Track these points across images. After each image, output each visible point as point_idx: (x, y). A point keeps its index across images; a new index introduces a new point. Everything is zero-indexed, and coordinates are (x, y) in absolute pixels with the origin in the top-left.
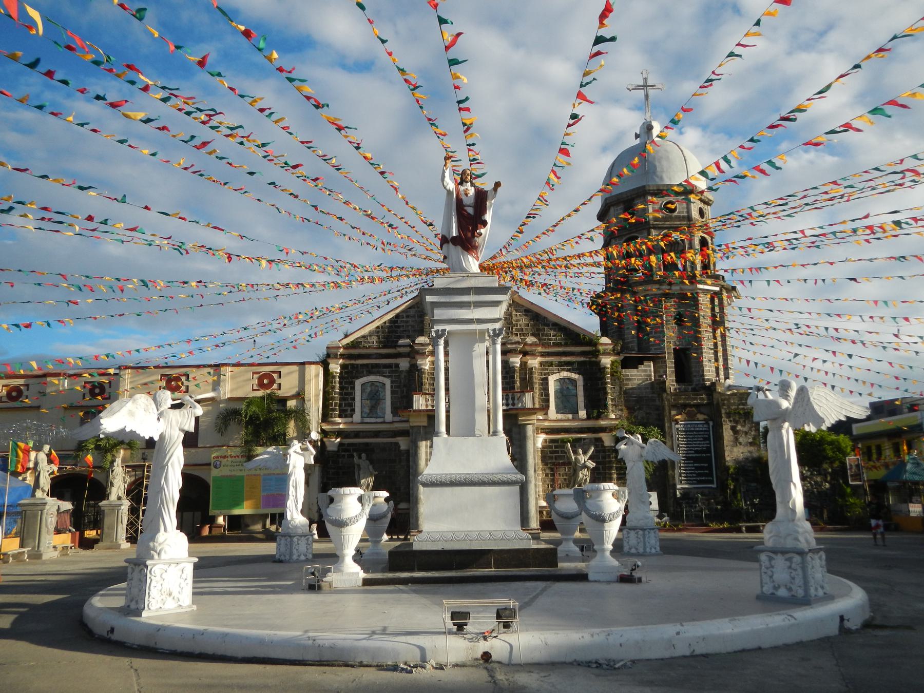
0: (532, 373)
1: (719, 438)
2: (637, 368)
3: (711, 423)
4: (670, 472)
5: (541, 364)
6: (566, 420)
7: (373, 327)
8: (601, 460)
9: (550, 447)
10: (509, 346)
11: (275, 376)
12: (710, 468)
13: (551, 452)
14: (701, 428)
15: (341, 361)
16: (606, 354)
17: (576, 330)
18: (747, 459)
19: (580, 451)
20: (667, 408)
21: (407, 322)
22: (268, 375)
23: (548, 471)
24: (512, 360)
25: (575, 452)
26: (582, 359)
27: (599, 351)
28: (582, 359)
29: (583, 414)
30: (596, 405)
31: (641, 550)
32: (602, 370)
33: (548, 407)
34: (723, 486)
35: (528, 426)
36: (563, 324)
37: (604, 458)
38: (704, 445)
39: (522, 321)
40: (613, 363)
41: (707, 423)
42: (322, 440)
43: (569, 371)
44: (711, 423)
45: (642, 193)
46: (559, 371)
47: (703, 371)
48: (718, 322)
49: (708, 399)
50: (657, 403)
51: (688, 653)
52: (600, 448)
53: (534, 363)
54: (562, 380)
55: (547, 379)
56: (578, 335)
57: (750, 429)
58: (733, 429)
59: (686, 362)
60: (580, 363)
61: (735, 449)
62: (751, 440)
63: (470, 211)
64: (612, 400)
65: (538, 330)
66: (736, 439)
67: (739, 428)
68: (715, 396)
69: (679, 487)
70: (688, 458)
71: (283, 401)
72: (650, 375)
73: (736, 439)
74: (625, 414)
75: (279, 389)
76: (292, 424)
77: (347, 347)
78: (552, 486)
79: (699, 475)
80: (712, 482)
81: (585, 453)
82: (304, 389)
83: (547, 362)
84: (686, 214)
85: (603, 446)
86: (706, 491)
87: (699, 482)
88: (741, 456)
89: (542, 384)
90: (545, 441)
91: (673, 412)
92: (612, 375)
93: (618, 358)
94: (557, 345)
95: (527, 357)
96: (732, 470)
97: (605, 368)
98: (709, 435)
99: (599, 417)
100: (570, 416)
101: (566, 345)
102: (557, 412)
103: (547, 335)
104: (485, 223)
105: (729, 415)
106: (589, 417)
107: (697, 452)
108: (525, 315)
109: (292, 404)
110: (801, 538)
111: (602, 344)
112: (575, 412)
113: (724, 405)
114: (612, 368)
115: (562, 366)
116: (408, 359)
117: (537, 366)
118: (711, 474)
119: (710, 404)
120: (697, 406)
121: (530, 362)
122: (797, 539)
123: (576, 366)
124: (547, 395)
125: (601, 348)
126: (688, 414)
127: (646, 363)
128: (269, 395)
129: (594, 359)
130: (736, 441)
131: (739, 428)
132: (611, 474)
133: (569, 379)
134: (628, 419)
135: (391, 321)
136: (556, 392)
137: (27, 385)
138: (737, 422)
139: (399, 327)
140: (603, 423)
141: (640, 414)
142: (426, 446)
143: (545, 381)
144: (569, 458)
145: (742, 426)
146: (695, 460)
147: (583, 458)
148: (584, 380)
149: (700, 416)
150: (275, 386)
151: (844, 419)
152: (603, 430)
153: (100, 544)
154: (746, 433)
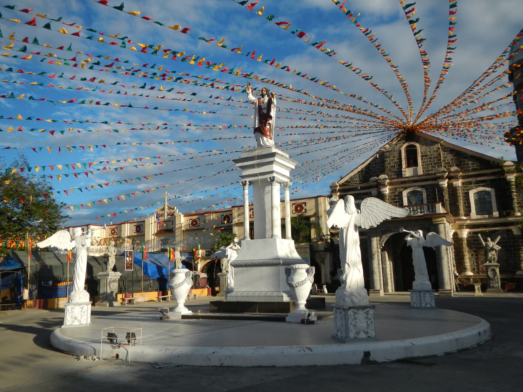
0: (456, 190)
5: (463, 183)
6: (484, 219)
7: (356, 171)
10: (438, 175)
11: (303, 205)
13: (474, 240)
15: (338, 194)
16: (510, 172)
17: (487, 158)
19: (489, 239)
21: (375, 167)
22: (300, 205)
23: (474, 253)
24: (441, 183)
25: (486, 240)
26: (493, 177)
27: (504, 171)
28: (493, 177)
29: (496, 214)
30: (506, 207)
31: (419, 305)
32: (508, 183)
33: (470, 211)
35: (440, 225)
36: (477, 155)
39: (450, 157)
40: (516, 178)
42: (331, 239)
43: (483, 186)
46: (476, 187)
51: (218, 364)
53: (459, 183)
54: (478, 193)
55: (468, 193)
56: (489, 162)
63: (265, 111)
64: (518, 203)
65: (460, 162)
71: (308, 218)
75: (306, 212)
76: (313, 231)
77: (340, 186)
78: (476, 262)
81: (493, 240)
82: (318, 211)
83: (467, 182)
89: (465, 197)
90: (470, 233)
94: (474, 170)
95: (452, 180)
97: (510, 182)
99: (508, 215)
100: (487, 216)
101: (481, 169)
102: (477, 214)
103: (467, 164)
104: (271, 118)
106: (501, 216)
108: (451, 153)
109: (313, 219)
110: (347, 299)
112: (490, 213)
114: (516, 182)
115: (478, 183)
116: (376, 189)
117: (460, 185)
121: (454, 183)
122: (344, 300)
123: (489, 182)
124: (469, 203)
125: (505, 169)
128: (300, 215)
129: (502, 177)
133: (484, 191)
135: (366, 167)
136: (476, 201)
137: (199, 218)
139: (371, 170)
140: (510, 219)
142: (377, 240)
143: (467, 196)
144: (481, 244)
147: (491, 244)
150: (304, 211)
151: (389, 218)
153: (219, 294)
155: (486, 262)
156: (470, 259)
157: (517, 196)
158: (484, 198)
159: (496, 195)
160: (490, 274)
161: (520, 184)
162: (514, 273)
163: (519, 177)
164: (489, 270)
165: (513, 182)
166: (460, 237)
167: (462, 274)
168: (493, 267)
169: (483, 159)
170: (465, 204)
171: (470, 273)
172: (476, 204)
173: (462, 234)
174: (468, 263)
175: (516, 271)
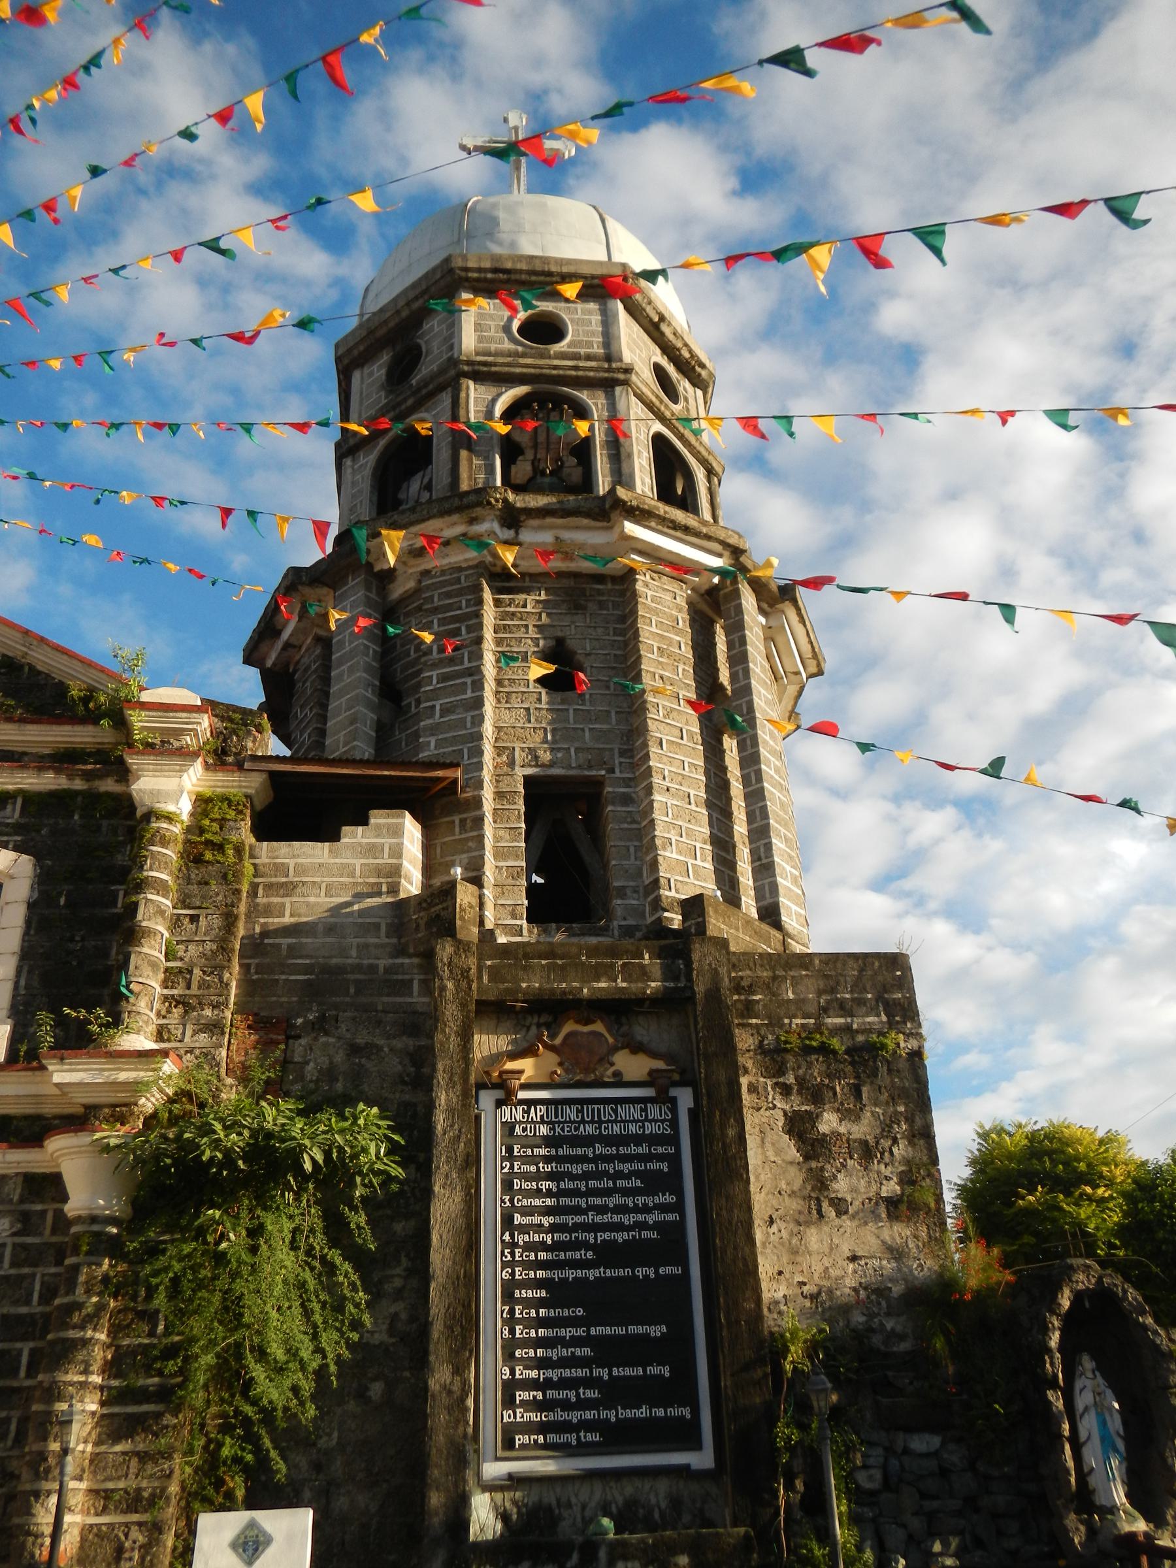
1: (723, 1168)
2: (335, 837)
3: (685, 1098)
4: (440, 1376)
12: (677, 1346)
14: (629, 1121)
18: (878, 1291)
20: (451, 1012)
32: (131, 823)
34: (748, 1461)
38: (645, 1217)
40: (203, 803)
41: (664, 1099)
44: (685, 1098)
45: (446, 284)
47: (654, 865)
48: (722, 711)
49: (669, 974)
50: (417, 998)
52: (47, 1236)
57: (886, 1129)
58: (799, 1127)
59: (580, 831)
60: (33, 801)
61: (814, 1238)
62: (891, 1188)
66: (819, 1184)
67: (829, 1122)
68: (701, 956)
69: (493, 1469)
70: (558, 1293)
72: (395, 872)
73: (819, 1184)
74: (235, 1046)
79: (614, 1393)
80: (687, 1436)
84: (598, 350)
85: (62, 1223)
86: (658, 1494)
87: (619, 1437)
88: (848, 1279)
91: (487, 1043)
92: (193, 856)
93: (244, 785)
96: (795, 1352)
98: (675, 1161)
105: (774, 1058)
107: (607, 1254)
111: (144, 706)
113: (748, 1009)
114: (194, 828)
118: (680, 1388)
119: (674, 1001)
120: (615, 1009)
125: (139, 721)
126: (567, 1052)
127: (378, 818)
129: (108, 785)
130: (818, 1196)
131: (829, 1122)
132: (53, 1393)
134: (244, 1080)
138: (816, 1096)
141: (316, 1055)
145: (846, 1115)
146: (597, 1301)
148: (44, 880)
149: (633, 1065)
152: (78, 1120)
154: (867, 1152)
157: (176, 923)
159: (31, 906)
161: (220, 848)
163: (225, 799)
165: (169, 818)
169: (32, 668)
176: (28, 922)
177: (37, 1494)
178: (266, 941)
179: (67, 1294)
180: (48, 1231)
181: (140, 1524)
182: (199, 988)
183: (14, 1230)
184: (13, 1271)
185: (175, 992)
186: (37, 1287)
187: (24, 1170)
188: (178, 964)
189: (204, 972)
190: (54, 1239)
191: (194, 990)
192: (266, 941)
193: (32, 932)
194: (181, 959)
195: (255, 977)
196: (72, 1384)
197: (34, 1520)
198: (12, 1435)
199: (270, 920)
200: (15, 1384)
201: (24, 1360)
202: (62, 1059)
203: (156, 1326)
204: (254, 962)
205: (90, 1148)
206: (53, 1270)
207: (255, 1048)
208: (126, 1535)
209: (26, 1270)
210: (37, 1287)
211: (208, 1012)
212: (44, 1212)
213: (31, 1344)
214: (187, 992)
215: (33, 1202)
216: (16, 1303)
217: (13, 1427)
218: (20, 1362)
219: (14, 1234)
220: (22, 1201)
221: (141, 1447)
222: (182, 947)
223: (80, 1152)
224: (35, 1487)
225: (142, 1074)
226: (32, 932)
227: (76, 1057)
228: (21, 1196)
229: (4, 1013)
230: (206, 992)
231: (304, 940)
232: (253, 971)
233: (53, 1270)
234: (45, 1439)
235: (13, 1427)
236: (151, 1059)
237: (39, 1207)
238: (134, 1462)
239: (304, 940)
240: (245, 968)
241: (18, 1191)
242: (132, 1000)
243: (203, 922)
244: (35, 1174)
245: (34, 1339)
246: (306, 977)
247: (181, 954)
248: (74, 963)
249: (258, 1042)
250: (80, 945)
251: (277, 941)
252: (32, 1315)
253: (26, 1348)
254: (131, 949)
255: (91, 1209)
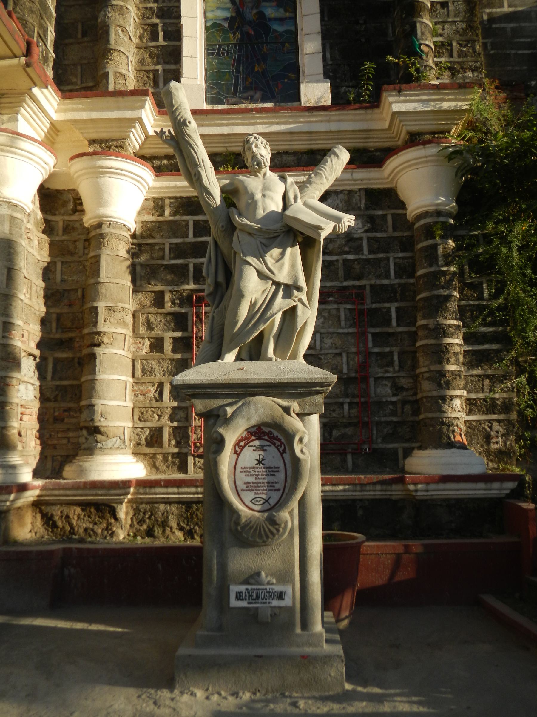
8: (393, 280)
9: (173, 229)
13: (178, 251)
37: (401, 271)
85: (401, 221)
90: (157, 204)
106: (339, 100)
124: (175, 34)
136: (212, 29)
155: (218, 356)
156: (141, 372)
158: (261, 15)
160: (237, 465)
162: (390, 461)
164: (231, 436)
166: (88, 220)
167: (69, 471)
168: (263, 407)
170: (154, 37)
171: (119, 465)
172: (212, 50)
173: (100, 198)
174: (118, 392)
175: (408, 453)
176: (322, 12)
177: (444, 398)
178: (494, 26)
179: (431, 266)
180: (390, 229)
181: (499, 421)
182: (459, 56)
183: (366, 228)
184: (371, 256)
185: (443, 59)
186: (392, 267)
187: (365, 187)
188: (440, 39)
189: (461, 45)
190: (396, 234)
191: (456, 59)
192: (494, 26)
193: (326, 19)
194: (441, 35)
195: (492, 52)
196: (450, 326)
197: (446, 415)
198: (396, 363)
199: (494, 10)
200: (390, 330)
201: (394, 315)
202: (399, 91)
203: (482, 293)
204: (488, 41)
205: (437, 158)
206: (401, 255)
207: (505, 103)
208: (491, 428)
209: (381, 255)
210: (392, 267)
211: (470, 74)
212: (384, 216)
213: (396, 304)
214: (451, 59)
215: (375, 209)
216: (379, 277)
217: (396, 358)
218: (390, 316)
219: (366, 231)
220: (367, 208)
221: (490, 372)
222: (439, 26)
223: (427, 162)
224: (442, 393)
225: (460, 103)
226: (326, 19)
227: (410, 89)
228: (366, 205)
229: (322, 76)
230: (465, 59)
231: (523, 25)
232: (489, 48)
233: (401, 255)
234: (441, 363)
235: (396, 358)
236: (467, 90)
237: (380, 212)
238: (487, 382)
239: (523, 25)
240: (484, 45)
241: (363, 201)
242: (424, 57)
243: (451, 7)
244: (372, 189)
245: (397, 301)
246: (530, 52)
247: (440, 31)
248: (363, 40)
249: (507, 99)
250: (363, 27)
251: (503, 25)
252: (392, 285)
253: (393, 307)
254: (415, 19)
255: (438, 205)
